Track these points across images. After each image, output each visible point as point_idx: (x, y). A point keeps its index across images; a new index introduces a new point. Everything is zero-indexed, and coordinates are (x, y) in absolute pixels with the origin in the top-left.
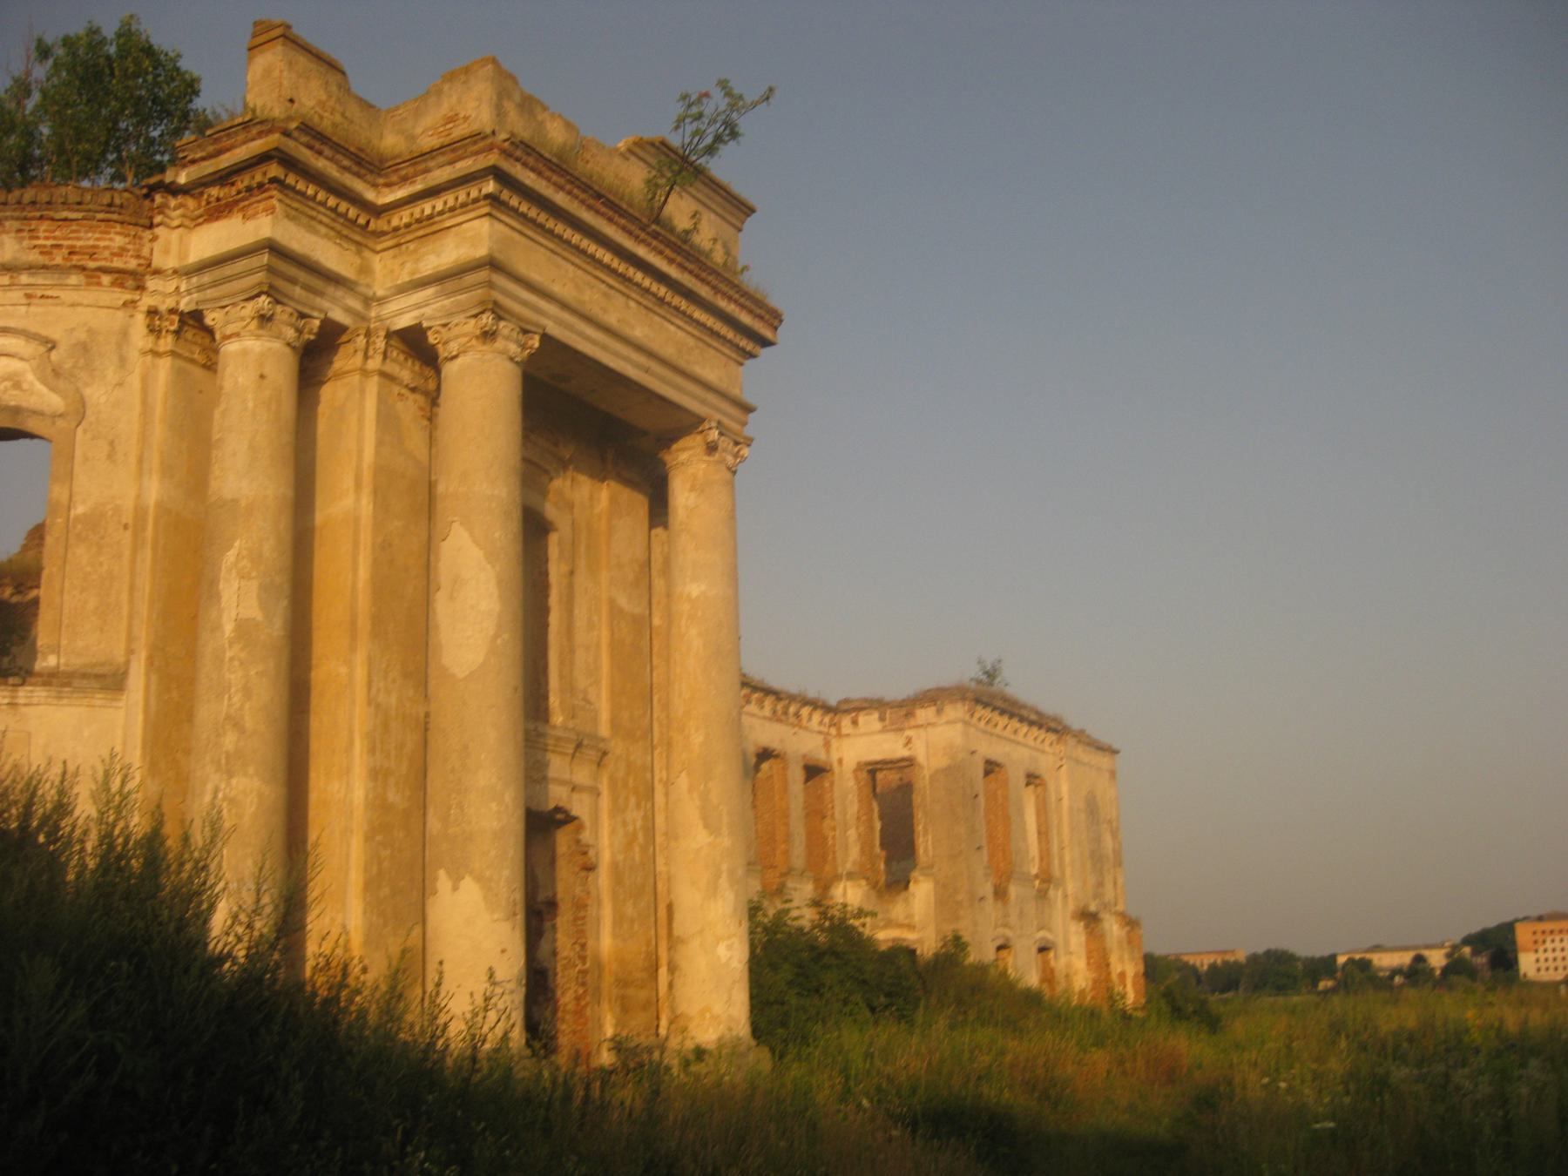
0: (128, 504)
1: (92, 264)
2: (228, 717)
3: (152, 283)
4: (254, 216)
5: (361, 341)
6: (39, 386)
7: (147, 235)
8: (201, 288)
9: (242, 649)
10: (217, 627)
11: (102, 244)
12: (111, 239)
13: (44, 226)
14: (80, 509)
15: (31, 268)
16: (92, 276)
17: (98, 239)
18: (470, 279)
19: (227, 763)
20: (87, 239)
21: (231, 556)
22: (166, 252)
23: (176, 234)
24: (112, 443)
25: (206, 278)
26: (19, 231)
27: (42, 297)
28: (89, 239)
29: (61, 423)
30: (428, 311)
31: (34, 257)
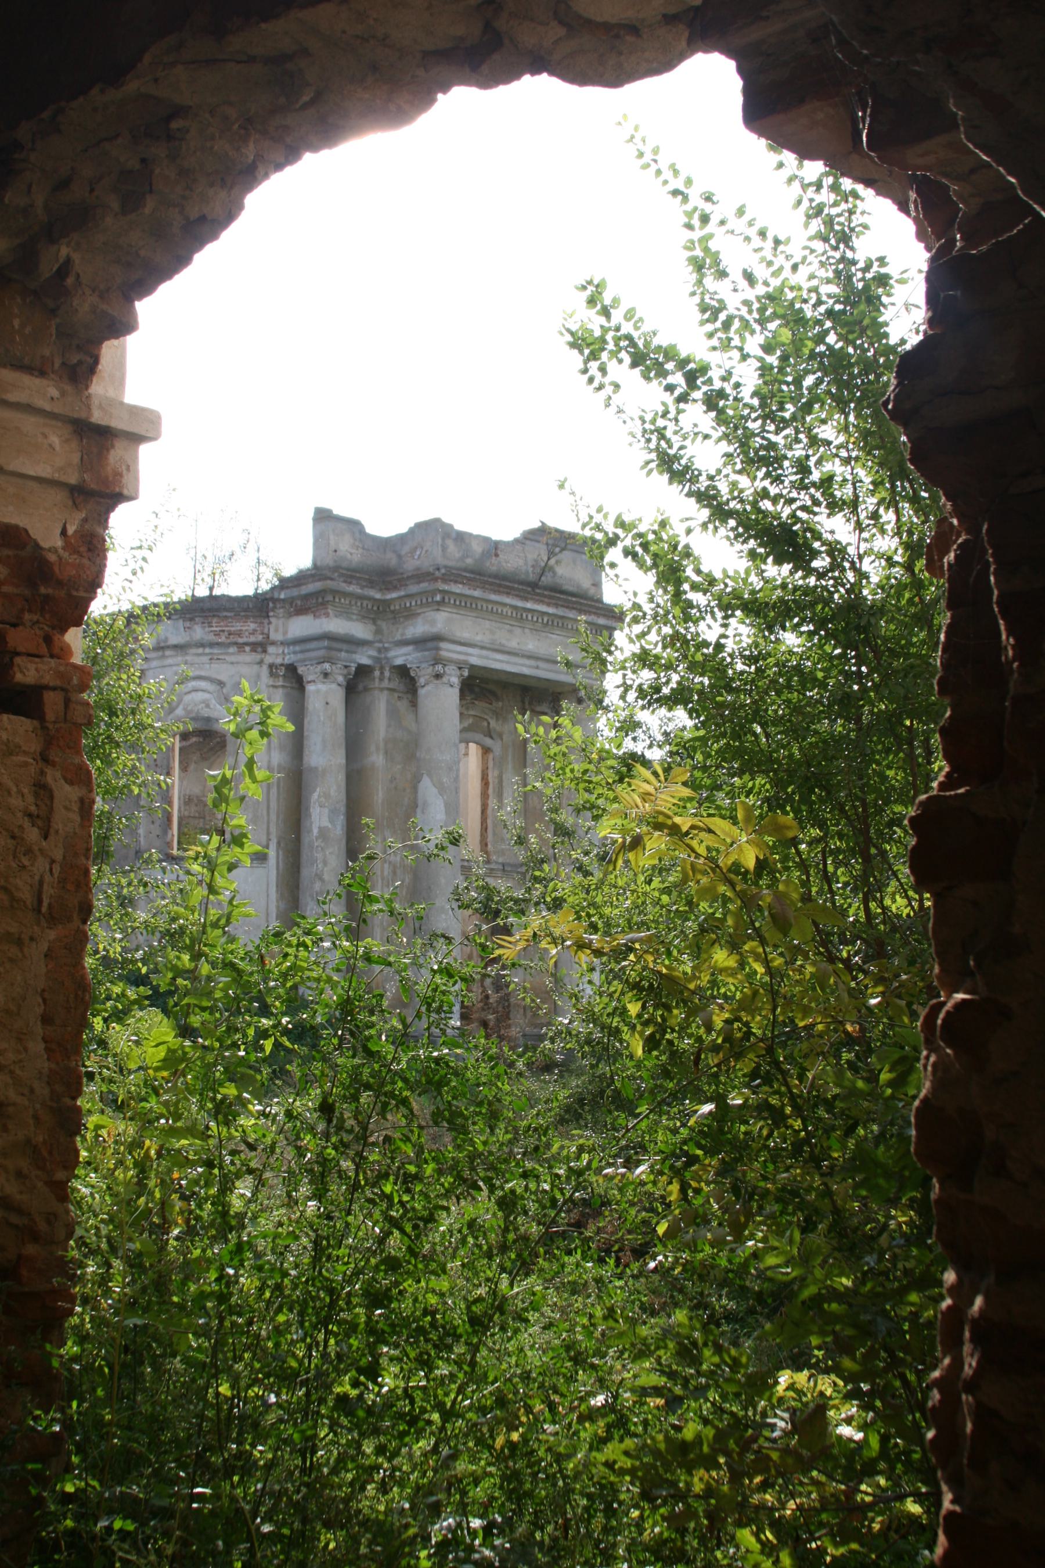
1: (240, 641)
3: (271, 649)
4: (319, 617)
5: (377, 673)
7: (266, 621)
8: (295, 653)
10: (310, 831)
13: (215, 620)
15: (212, 645)
16: (241, 646)
18: (430, 645)
20: (237, 626)
21: (315, 796)
22: (276, 630)
23: (281, 622)
25: (297, 648)
30: (410, 658)
31: (212, 638)
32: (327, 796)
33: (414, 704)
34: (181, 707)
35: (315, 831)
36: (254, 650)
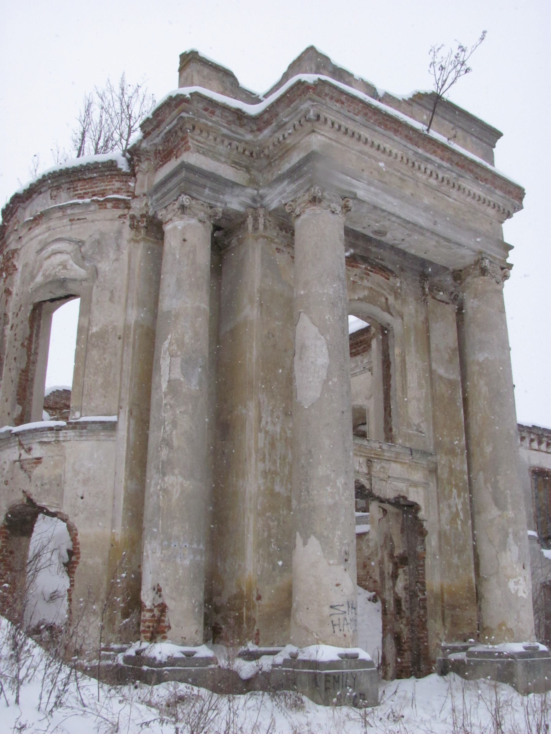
0: (120, 325)
2: (164, 440)
6: (76, 267)
9: (171, 399)
10: (160, 386)
11: (108, 187)
12: (113, 185)
14: (94, 329)
17: (106, 186)
19: (162, 467)
21: (166, 344)
24: (112, 292)
26: (69, 189)
27: (78, 219)
28: (102, 186)
29: (85, 284)
32: (181, 343)
33: (291, 244)
34: (41, 273)
35: (164, 386)
36: (116, 207)
